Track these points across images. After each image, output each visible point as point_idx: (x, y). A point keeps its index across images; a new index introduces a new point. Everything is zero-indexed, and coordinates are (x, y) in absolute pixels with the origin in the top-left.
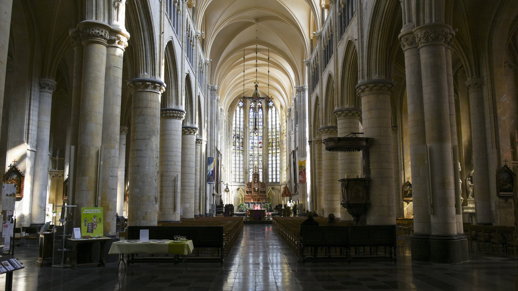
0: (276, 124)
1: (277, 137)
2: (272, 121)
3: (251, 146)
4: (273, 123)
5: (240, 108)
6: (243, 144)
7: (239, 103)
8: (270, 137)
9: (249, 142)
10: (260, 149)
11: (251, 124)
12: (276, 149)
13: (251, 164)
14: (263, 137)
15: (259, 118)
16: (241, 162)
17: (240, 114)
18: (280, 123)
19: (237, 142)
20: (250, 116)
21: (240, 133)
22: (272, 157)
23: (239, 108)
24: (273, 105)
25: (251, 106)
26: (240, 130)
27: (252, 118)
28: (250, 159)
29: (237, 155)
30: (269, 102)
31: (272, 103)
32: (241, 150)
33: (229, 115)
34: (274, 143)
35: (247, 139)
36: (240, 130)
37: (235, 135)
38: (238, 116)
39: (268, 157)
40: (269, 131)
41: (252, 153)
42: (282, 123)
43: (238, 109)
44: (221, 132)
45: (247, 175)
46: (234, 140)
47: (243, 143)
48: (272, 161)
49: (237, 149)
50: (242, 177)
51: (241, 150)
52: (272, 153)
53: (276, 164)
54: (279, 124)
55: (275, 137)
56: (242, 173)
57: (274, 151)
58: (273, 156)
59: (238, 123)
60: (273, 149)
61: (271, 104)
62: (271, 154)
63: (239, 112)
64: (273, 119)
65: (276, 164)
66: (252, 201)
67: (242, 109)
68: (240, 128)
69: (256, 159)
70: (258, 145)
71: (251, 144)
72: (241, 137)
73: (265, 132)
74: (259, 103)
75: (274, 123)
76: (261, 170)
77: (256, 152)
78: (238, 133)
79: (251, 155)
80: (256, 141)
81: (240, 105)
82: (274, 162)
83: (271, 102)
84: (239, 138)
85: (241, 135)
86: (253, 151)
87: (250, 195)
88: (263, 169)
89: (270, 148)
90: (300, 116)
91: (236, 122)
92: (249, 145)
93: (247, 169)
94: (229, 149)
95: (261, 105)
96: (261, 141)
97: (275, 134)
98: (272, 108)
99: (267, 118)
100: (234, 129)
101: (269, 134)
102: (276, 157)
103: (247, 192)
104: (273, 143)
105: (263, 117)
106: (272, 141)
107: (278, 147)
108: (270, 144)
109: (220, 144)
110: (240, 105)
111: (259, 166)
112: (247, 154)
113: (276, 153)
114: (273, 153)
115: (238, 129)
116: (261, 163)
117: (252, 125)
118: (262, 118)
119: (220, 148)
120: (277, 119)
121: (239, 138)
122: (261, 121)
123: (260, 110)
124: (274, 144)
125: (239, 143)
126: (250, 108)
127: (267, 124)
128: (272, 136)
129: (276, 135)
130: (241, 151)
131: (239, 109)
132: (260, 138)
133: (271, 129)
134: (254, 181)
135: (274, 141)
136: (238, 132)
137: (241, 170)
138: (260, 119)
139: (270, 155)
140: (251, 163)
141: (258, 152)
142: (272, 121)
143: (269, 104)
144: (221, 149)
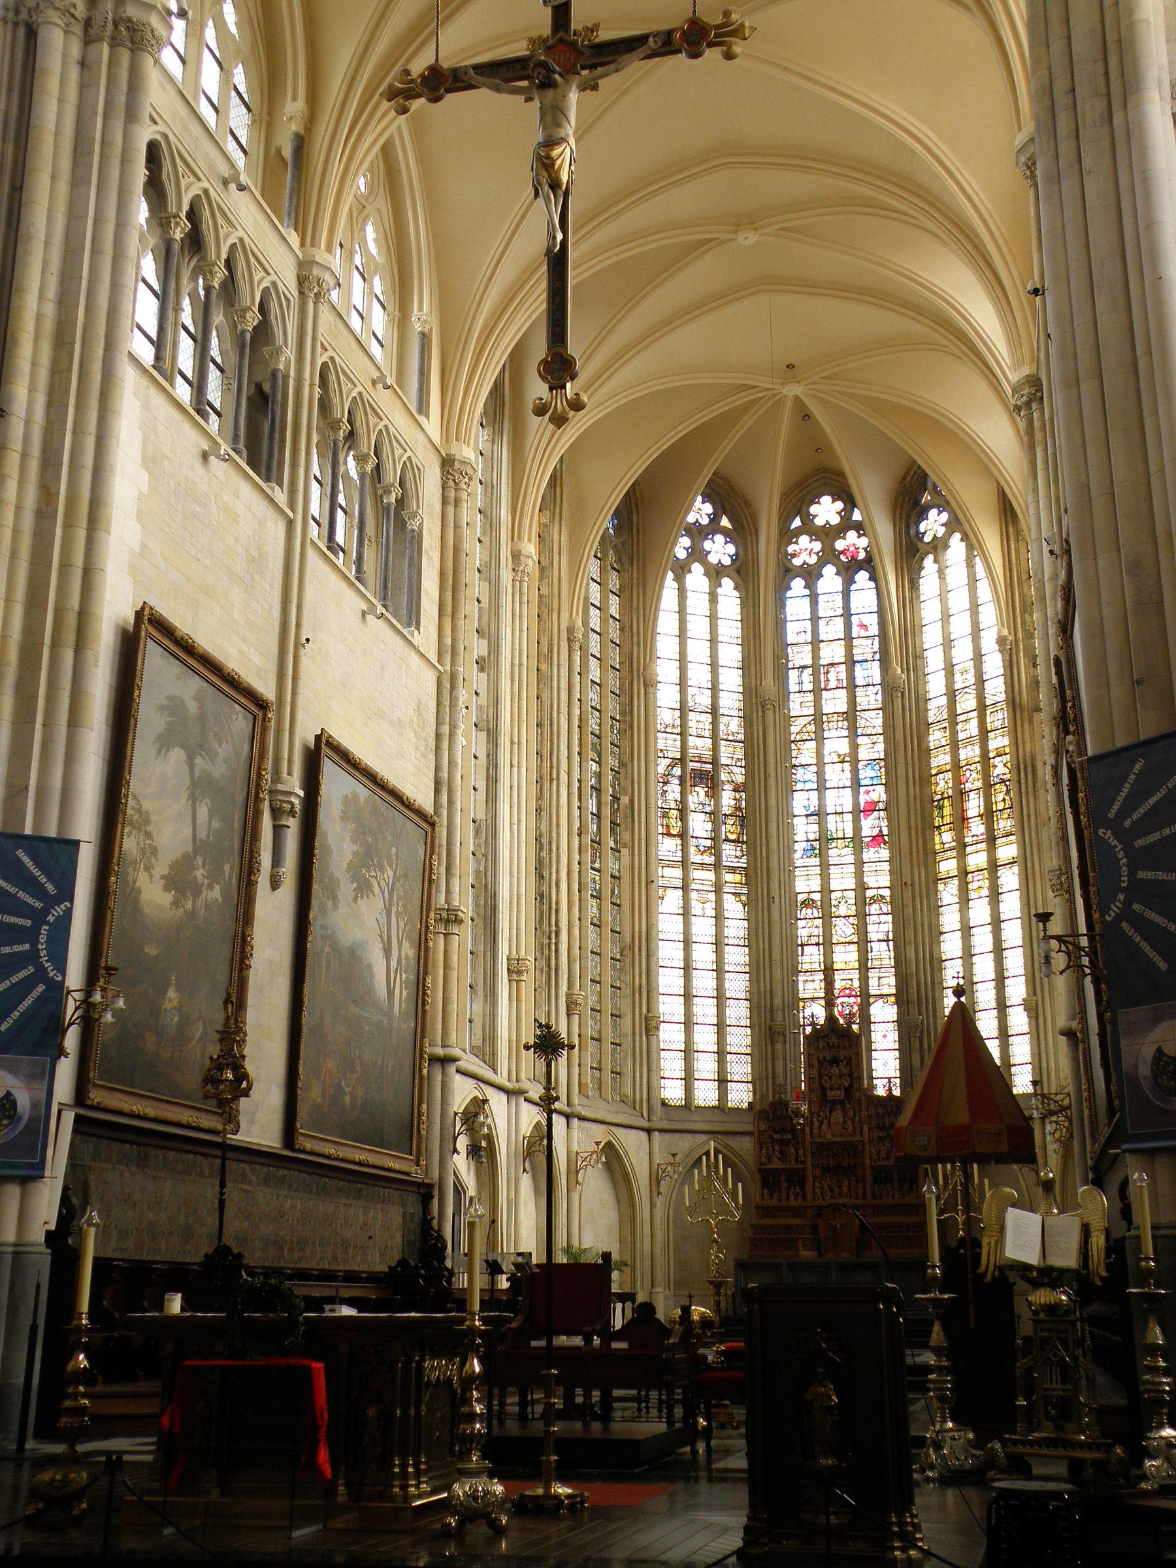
0: (978, 657)
2: (948, 644)
3: (800, 836)
5: (715, 573)
6: (742, 826)
7: (707, 545)
8: (941, 759)
9: (789, 806)
10: (868, 854)
11: (801, 683)
12: (991, 839)
14: (889, 761)
15: (855, 632)
16: (737, 957)
17: (713, 618)
18: (1005, 632)
19: (692, 806)
20: (791, 628)
21: (715, 749)
22: (964, 900)
23: (706, 574)
24: (953, 525)
25: (797, 562)
26: (715, 723)
27: (801, 639)
29: (696, 908)
30: (922, 514)
31: (944, 517)
32: (733, 870)
33: (625, 619)
35: (772, 781)
36: (715, 723)
37: (682, 760)
38: (698, 627)
39: (935, 909)
41: (815, 884)
42: (1020, 636)
43: (697, 578)
44: (448, 641)
45: (779, 1046)
46: (670, 796)
47: (743, 818)
48: (966, 930)
49: (695, 857)
50: (740, 1068)
51: (733, 870)
52: (963, 873)
53: (998, 950)
54: (1001, 641)
56: (740, 1039)
57: (977, 859)
58: (972, 895)
59: (699, 675)
60: (965, 846)
61: (933, 524)
62: (956, 881)
63: (706, 604)
64: (952, 628)
65: (998, 950)
66: (807, 1254)
67: (727, 584)
68: (714, 711)
69: (844, 929)
70: (857, 828)
72: (724, 777)
73: (899, 722)
74: (852, 535)
75: (962, 652)
76: (884, 1013)
77: (842, 880)
78: (700, 745)
79: (808, 904)
80: (839, 800)
81: (713, 559)
82: (983, 940)
83: (933, 513)
84: (710, 780)
85: (724, 761)
86: (825, 866)
87: (792, 1202)
88: (902, 998)
89: (948, 837)
90: (1062, 100)
91: (683, 669)
92: (790, 826)
93: (778, 1001)
94: (625, 852)
95: (864, 542)
96: (874, 796)
98: (946, 546)
99: (911, 629)
100: (668, 721)
101: (937, 737)
102: (995, 896)
103: (765, 1183)
104: (960, 795)
105: (882, 624)
106: (958, 781)
107: (1004, 824)
108: (947, 811)
109: (438, 737)
110: (713, 559)
111: (873, 982)
112: (777, 897)
113: (993, 866)
114: (967, 874)
115: (699, 722)
116: (885, 955)
117: (808, 686)
118: (874, 630)
119: (437, 769)
120: (981, 617)
121: (710, 780)
122: (870, 657)
123: (862, 577)
124: (974, 805)
125: (715, 816)
126: (786, 572)
127: (915, 669)
128: (955, 745)
129: (984, 732)
130: (729, 877)
131: (706, 580)
132: (866, 774)
133: (944, 701)
134: (823, 1090)
135: (973, 780)
136: (700, 742)
137: (738, 1012)
139: (948, 894)
140: (806, 959)
141: (859, 874)
142: (948, 644)
143: (923, 527)
144: (445, 774)
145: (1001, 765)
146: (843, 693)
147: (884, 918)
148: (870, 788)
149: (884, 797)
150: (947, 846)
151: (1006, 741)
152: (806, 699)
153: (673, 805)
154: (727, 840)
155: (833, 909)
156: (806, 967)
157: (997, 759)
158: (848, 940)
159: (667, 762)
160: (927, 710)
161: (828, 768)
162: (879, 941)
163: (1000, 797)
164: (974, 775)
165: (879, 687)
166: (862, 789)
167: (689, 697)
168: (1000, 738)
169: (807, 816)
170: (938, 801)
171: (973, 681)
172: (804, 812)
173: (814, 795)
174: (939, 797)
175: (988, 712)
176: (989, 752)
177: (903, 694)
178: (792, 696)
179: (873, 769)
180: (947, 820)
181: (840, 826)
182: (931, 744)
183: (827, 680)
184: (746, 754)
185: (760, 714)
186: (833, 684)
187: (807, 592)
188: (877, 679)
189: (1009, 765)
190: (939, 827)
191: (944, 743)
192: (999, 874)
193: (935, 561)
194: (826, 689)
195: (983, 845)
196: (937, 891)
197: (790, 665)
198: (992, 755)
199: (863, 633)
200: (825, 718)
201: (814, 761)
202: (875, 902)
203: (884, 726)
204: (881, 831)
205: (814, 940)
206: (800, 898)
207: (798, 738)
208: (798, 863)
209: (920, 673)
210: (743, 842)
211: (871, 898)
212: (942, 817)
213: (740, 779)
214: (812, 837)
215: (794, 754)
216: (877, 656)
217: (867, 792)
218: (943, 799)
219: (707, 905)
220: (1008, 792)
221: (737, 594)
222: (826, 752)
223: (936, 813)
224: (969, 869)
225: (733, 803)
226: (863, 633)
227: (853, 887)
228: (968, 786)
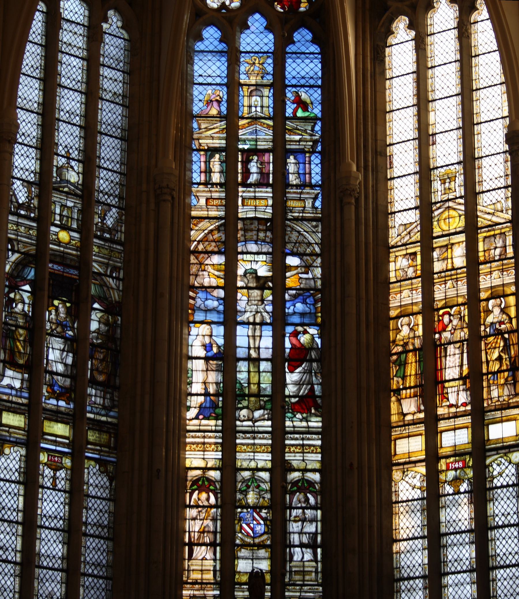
1: (485, 282)
3: (197, 388)
4: (433, 151)
11: (208, 171)
13: (202, 584)
28: (196, 526)
34: (451, 349)
40: (393, 239)
55: (463, 288)
60: (438, 419)
62: (422, 469)
63: (80, 42)
71: (199, 365)
85: (96, 267)
96: (304, 339)
97: (460, 261)
108: (412, 369)
114: (438, 459)
116: (310, 566)
117: (216, 178)
118: (317, 111)
130: (92, 436)
133: (413, 216)
136: (64, 236)
138: (301, 126)
140: (195, 565)
145: (497, 311)
146: (267, 193)
147: (309, 513)
148: (300, 329)
149: (318, 341)
150: (409, 418)
151: (510, 278)
152: (215, 195)
153: (21, 321)
154: (93, 382)
155: (239, 496)
156: (195, 576)
157: (491, 302)
158: (257, 541)
159: (14, 257)
160: (387, 228)
161: (242, 296)
162: (302, 545)
163: (496, 355)
164: (455, 322)
165: (318, 190)
166: (289, 329)
167: (55, 169)
168: (495, 274)
169: (207, 359)
170: (399, 354)
171: (460, 191)
172: (202, 353)
173: (220, 330)
174: (400, 349)
175: (481, 236)
176: (479, 291)
177: (357, 200)
178: (194, 189)
179: (304, 302)
180: (411, 381)
181: (254, 379)
182: (392, 274)
183: (247, 173)
184: (126, 262)
185: (152, 206)
186: (253, 178)
187: (222, 47)
188: (316, 179)
189: (513, 312)
190: (398, 391)
191: (410, 272)
192: (488, 462)
193: (411, 26)
194: (245, 184)
195: (467, 420)
196: (390, 479)
197: (195, 145)
198: (483, 295)
199: (300, 113)
200: (240, 225)
201: (221, 282)
202: (300, 490)
203: (322, 244)
204: (312, 390)
205: (207, 540)
206: (192, 474)
207: (201, 247)
208: (192, 425)
209: (381, 176)
210: (115, 388)
211: (295, 483)
212: (404, 378)
213: (116, 296)
214: (212, 389)
215: (194, 269)
216: (319, 148)
217: (295, 334)
218: (406, 352)
219: (61, 474)
220: (506, 348)
221: (126, 36)
222: (240, 272)
223: (394, 370)
224: (442, 452)
225: (103, 328)
226: (300, 113)
227: (269, 465)
228: (446, 335)
